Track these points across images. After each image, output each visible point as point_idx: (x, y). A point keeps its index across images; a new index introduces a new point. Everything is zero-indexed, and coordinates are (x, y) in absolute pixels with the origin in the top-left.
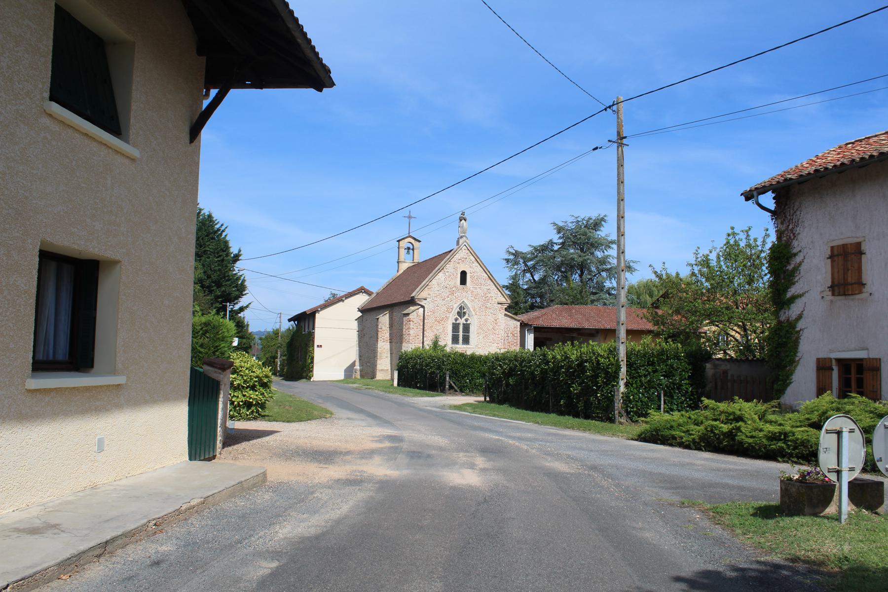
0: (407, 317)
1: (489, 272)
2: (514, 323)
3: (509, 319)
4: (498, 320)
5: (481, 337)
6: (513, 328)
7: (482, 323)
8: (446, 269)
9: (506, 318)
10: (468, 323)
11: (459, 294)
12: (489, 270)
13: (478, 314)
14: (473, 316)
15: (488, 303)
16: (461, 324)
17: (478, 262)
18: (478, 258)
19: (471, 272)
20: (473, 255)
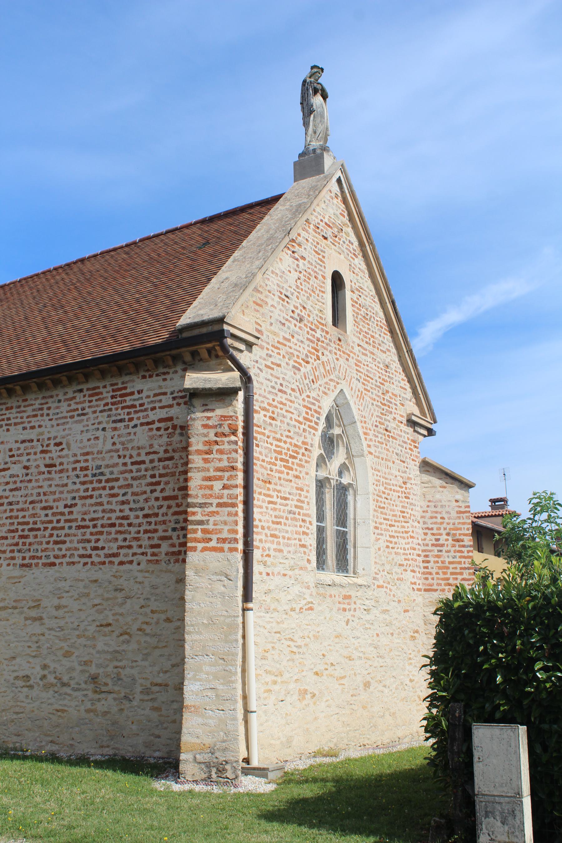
0: (219, 412)
1: (393, 303)
2: (458, 497)
3: (437, 482)
4: (408, 485)
5: (382, 544)
6: (454, 514)
7: (382, 488)
8: (299, 245)
9: (426, 477)
10: (345, 481)
11: (330, 356)
12: (394, 297)
13: (372, 450)
14: (362, 455)
15: (390, 417)
16: (333, 483)
17: (365, 256)
18: (371, 243)
19: (353, 284)
20: (354, 227)
